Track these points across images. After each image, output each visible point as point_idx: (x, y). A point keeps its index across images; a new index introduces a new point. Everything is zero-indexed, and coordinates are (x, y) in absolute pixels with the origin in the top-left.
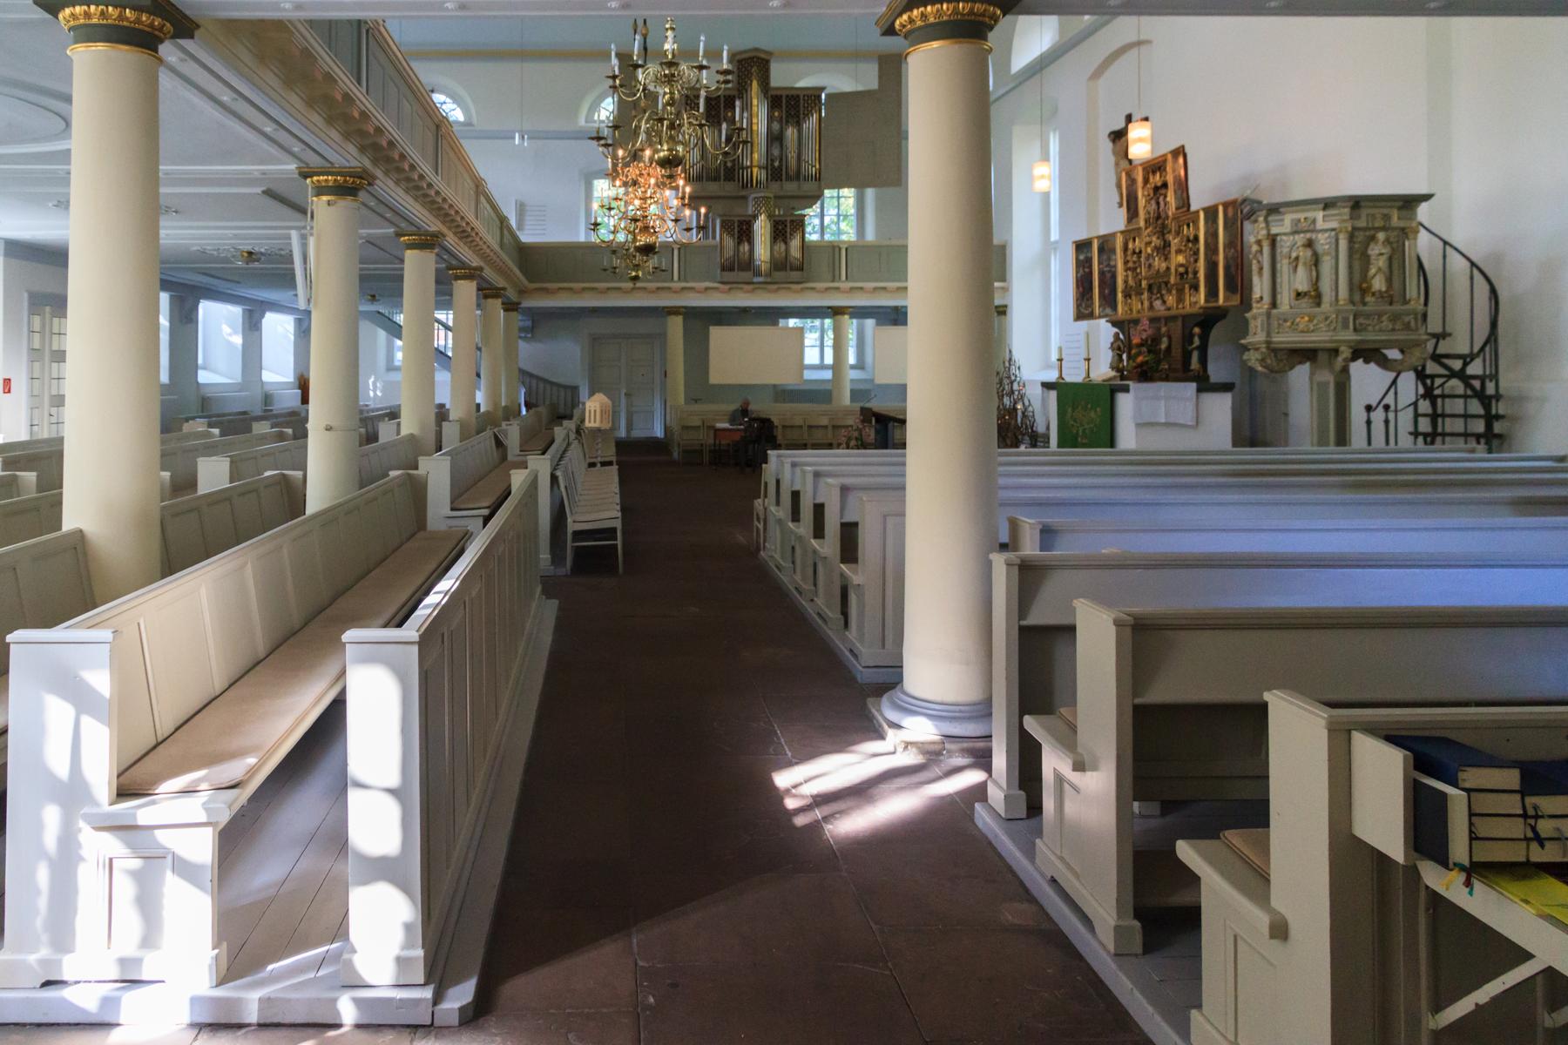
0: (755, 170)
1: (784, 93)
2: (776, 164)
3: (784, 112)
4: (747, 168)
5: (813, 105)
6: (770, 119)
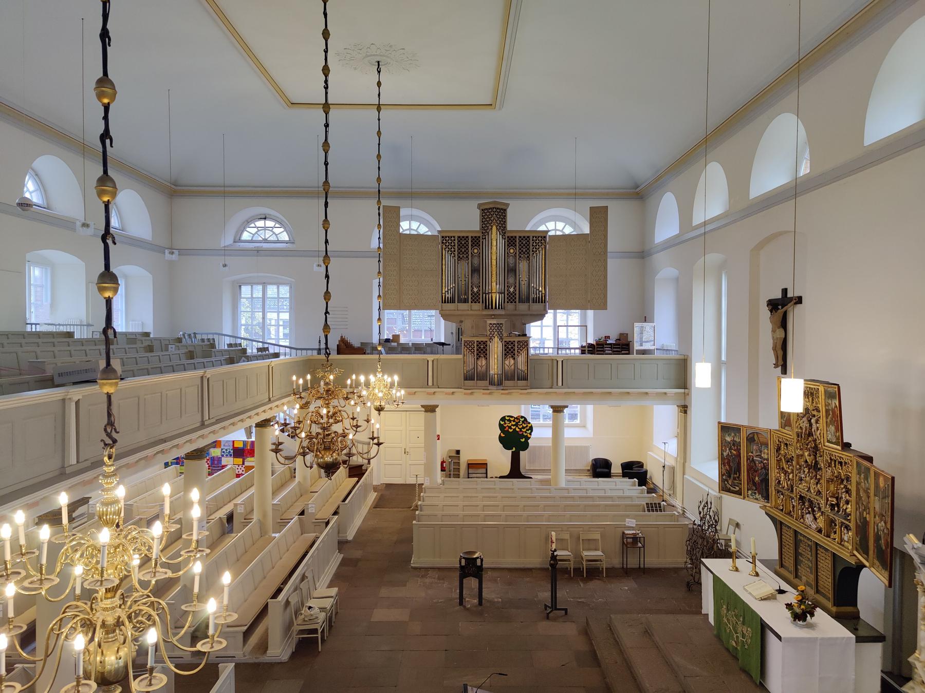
0: (494, 296)
1: (518, 235)
2: (512, 290)
4: (489, 293)
5: (540, 244)
6: (507, 255)
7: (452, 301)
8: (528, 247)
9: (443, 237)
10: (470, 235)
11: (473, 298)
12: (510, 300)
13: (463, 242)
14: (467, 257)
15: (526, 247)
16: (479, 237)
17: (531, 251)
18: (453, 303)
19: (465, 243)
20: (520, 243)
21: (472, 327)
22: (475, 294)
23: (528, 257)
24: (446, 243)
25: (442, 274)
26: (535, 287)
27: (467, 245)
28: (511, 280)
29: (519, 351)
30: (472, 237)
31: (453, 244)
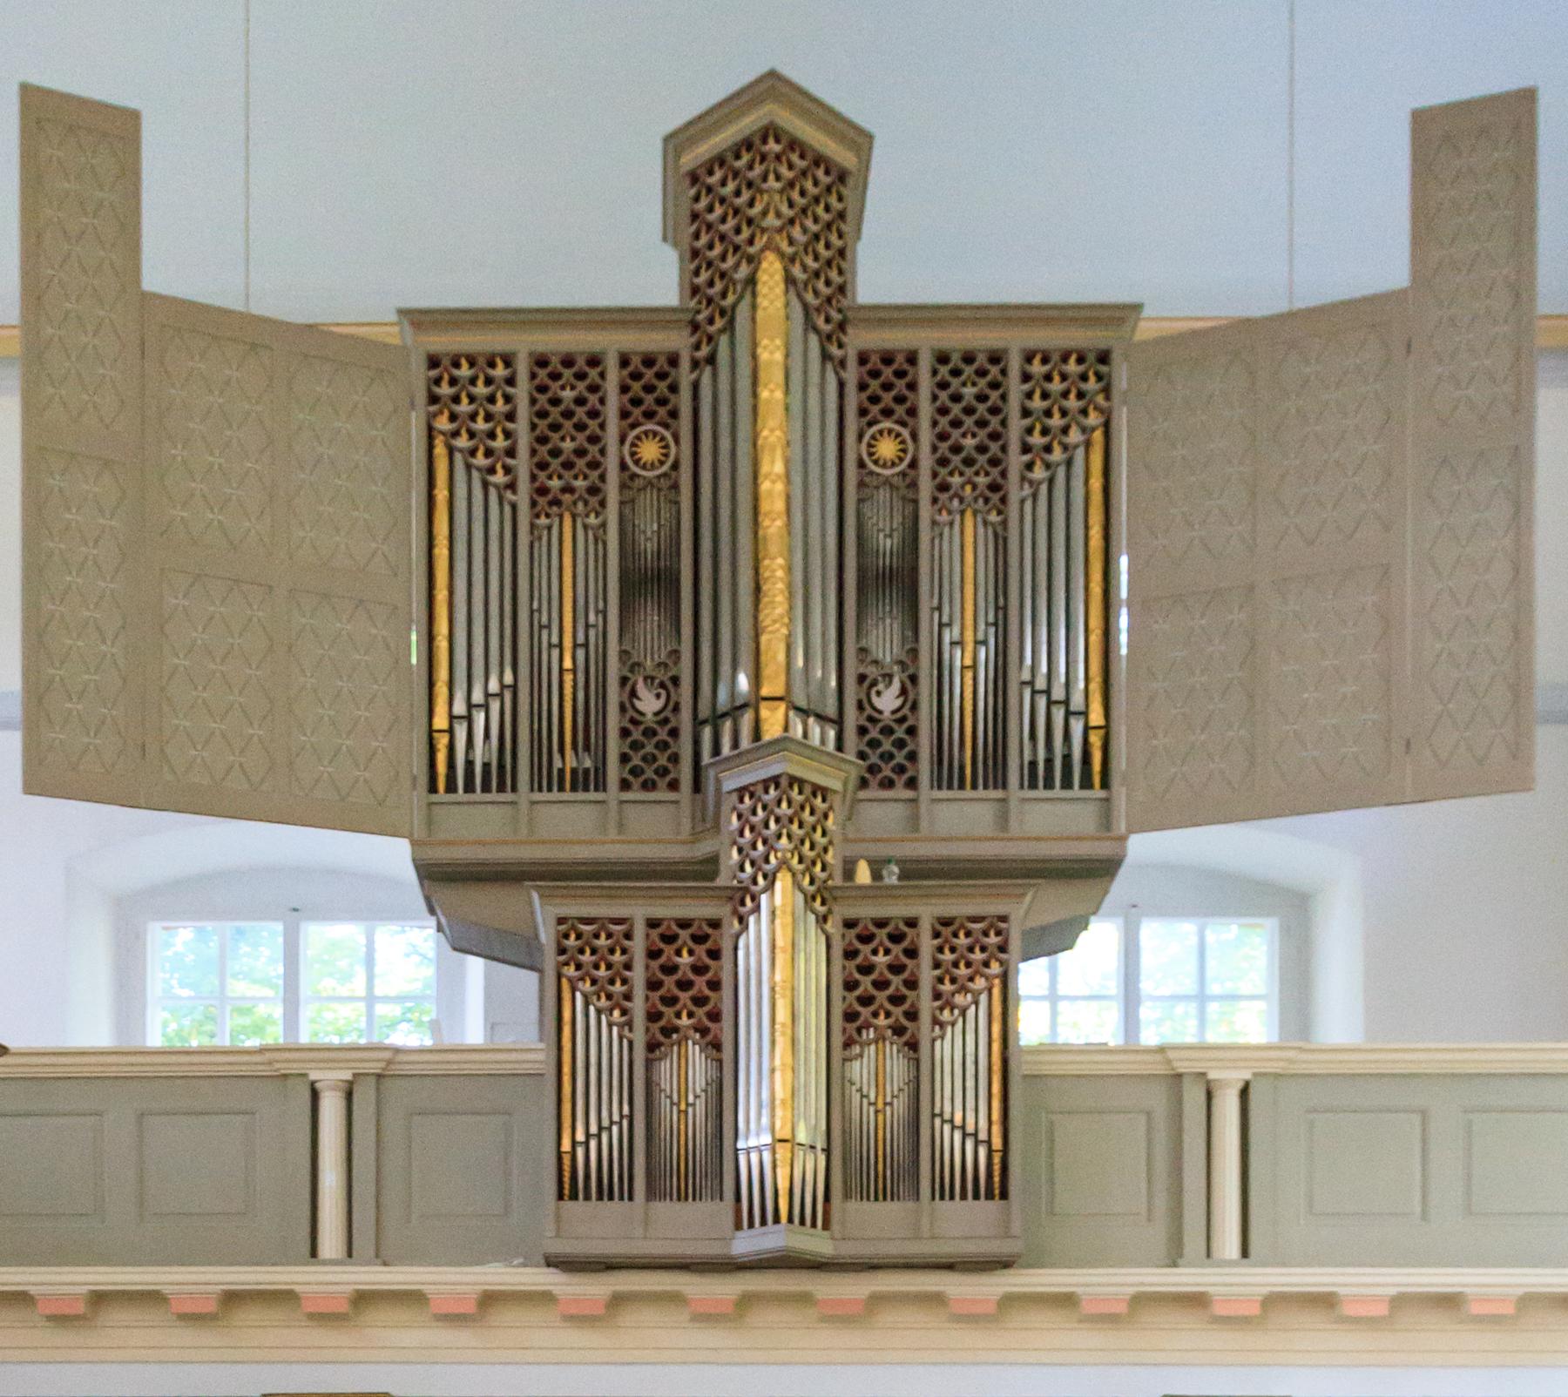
1: (926, 340)
2: (887, 701)
3: (926, 436)
4: (736, 710)
5: (1072, 403)
7: (499, 777)
8: (994, 422)
9: (433, 362)
10: (611, 343)
11: (636, 761)
14: (593, 490)
15: (982, 423)
16: (673, 360)
20: (944, 396)
22: (650, 733)
23: (994, 487)
24: (456, 399)
26: (1041, 684)
27: (594, 414)
28: (885, 641)
30: (624, 362)
31: (500, 406)
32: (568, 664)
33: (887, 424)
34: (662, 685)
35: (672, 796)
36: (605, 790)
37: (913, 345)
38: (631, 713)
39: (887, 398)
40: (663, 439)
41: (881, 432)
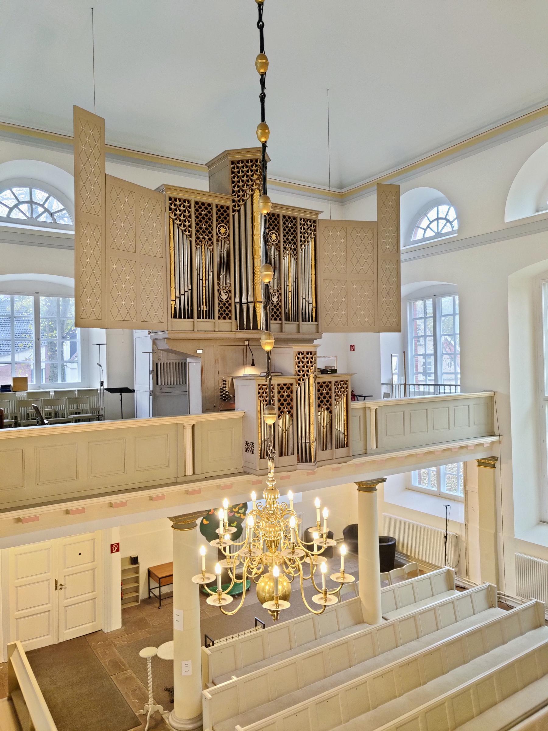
2: (275, 299)
12: (273, 316)
13: (203, 213)
14: (210, 239)
15: (292, 234)
16: (228, 208)
17: (299, 241)
18: (188, 318)
19: (206, 215)
21: (216, 361)
23: (295, 249)
24: (176, 210)
25: (171, 264)
27: (210, 219)
29: (337, 398)
31: (187, 214)
32: (204, 285)
33: (273, 231)
34: (227, 292)
35: (230, 321)
36: (214, 319)
37: (279, 213)
38: (220, 299)
39: (273, 224)
40: (226, 228)
41: (272, 233)
